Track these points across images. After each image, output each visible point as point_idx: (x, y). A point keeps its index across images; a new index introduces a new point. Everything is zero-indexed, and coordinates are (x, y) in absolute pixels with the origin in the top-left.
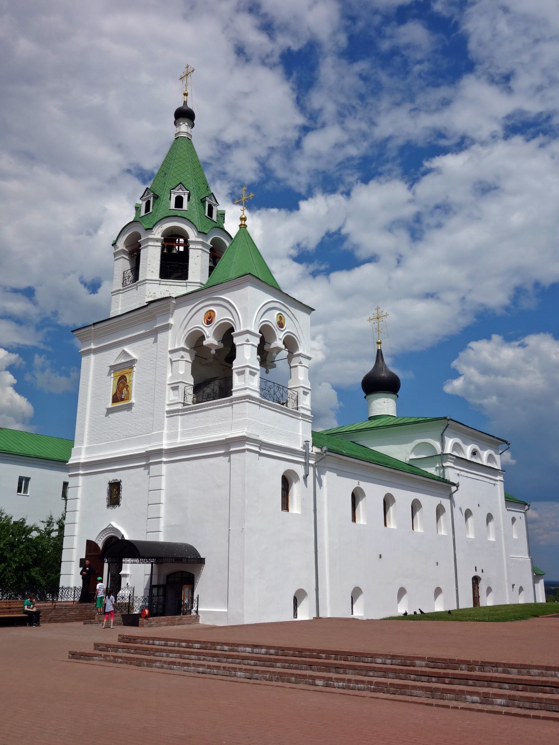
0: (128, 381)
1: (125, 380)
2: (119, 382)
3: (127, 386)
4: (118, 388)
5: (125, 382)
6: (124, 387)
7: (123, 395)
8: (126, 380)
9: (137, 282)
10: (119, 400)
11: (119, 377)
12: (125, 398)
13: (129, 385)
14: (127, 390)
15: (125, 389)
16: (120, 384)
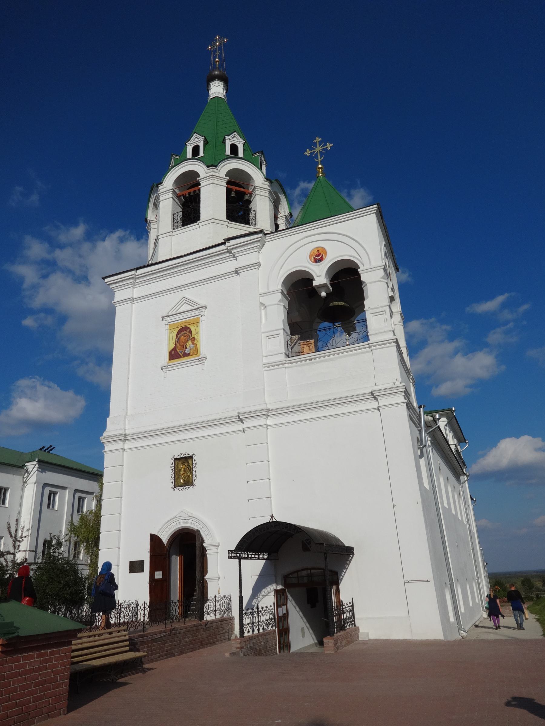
0: (193, 332)
1: (189, 332)
2: (180, 335)
3: (193, 339)
4: (178, 341)
5: (189, 334)
6: (188, 341)
7: (186, 350)
8: (190, 332)
9: (198, 222)
10: (180, 356)
11: (179, 328)
12: (192, 353)
13: (196, 337)
14: (193, 343)
15: (190, 343)
16: (180, 337)
